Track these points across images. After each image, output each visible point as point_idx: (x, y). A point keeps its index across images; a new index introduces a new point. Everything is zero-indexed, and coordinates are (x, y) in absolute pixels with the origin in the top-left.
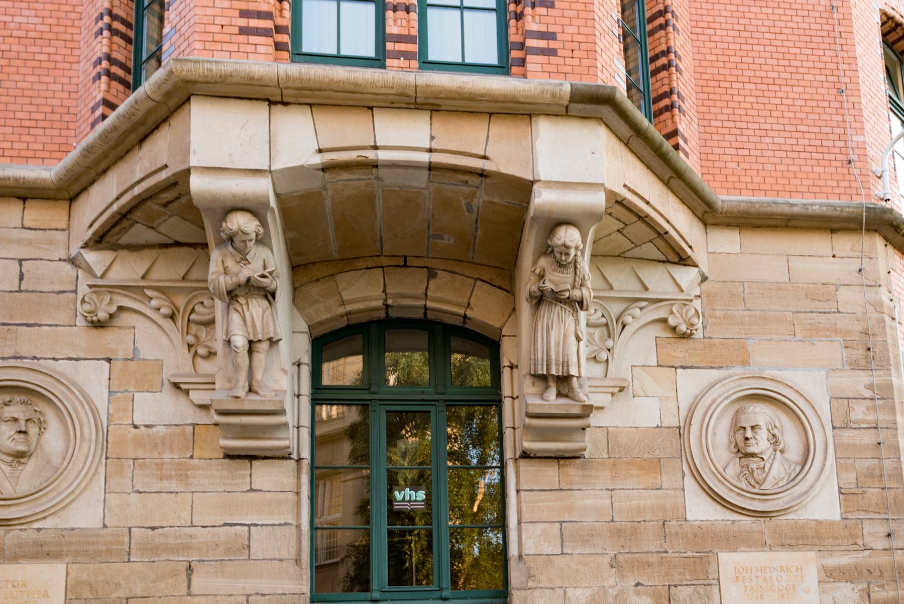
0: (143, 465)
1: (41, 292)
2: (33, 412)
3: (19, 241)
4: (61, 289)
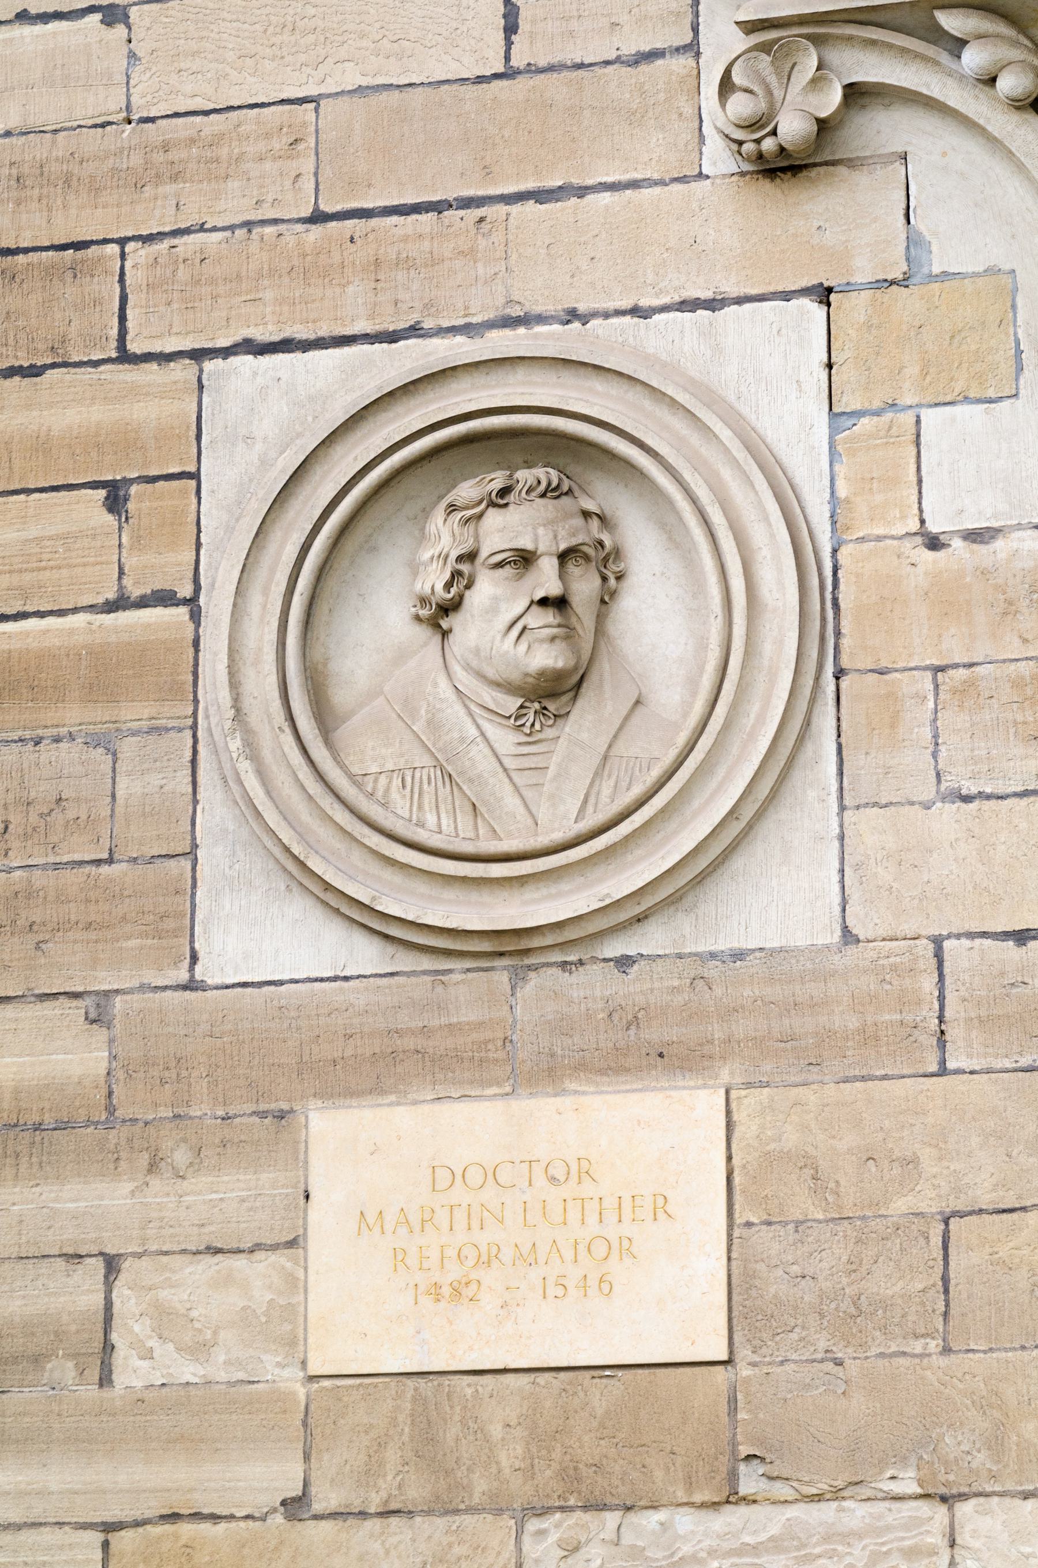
0: (963, 691)
1: (580, 66)
2: (579, 521)
4: (646, 48)
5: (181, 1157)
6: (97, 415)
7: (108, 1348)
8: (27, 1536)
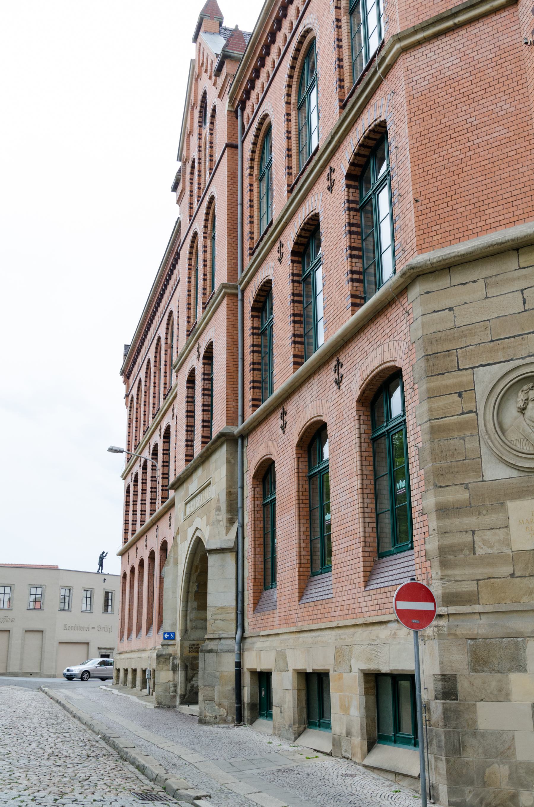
3: (519, 278)
5: (484, 512)
6: (455, 380)
7: (474, 548)
8: (462, 582)
